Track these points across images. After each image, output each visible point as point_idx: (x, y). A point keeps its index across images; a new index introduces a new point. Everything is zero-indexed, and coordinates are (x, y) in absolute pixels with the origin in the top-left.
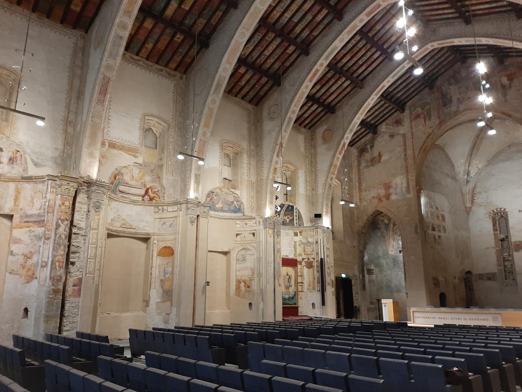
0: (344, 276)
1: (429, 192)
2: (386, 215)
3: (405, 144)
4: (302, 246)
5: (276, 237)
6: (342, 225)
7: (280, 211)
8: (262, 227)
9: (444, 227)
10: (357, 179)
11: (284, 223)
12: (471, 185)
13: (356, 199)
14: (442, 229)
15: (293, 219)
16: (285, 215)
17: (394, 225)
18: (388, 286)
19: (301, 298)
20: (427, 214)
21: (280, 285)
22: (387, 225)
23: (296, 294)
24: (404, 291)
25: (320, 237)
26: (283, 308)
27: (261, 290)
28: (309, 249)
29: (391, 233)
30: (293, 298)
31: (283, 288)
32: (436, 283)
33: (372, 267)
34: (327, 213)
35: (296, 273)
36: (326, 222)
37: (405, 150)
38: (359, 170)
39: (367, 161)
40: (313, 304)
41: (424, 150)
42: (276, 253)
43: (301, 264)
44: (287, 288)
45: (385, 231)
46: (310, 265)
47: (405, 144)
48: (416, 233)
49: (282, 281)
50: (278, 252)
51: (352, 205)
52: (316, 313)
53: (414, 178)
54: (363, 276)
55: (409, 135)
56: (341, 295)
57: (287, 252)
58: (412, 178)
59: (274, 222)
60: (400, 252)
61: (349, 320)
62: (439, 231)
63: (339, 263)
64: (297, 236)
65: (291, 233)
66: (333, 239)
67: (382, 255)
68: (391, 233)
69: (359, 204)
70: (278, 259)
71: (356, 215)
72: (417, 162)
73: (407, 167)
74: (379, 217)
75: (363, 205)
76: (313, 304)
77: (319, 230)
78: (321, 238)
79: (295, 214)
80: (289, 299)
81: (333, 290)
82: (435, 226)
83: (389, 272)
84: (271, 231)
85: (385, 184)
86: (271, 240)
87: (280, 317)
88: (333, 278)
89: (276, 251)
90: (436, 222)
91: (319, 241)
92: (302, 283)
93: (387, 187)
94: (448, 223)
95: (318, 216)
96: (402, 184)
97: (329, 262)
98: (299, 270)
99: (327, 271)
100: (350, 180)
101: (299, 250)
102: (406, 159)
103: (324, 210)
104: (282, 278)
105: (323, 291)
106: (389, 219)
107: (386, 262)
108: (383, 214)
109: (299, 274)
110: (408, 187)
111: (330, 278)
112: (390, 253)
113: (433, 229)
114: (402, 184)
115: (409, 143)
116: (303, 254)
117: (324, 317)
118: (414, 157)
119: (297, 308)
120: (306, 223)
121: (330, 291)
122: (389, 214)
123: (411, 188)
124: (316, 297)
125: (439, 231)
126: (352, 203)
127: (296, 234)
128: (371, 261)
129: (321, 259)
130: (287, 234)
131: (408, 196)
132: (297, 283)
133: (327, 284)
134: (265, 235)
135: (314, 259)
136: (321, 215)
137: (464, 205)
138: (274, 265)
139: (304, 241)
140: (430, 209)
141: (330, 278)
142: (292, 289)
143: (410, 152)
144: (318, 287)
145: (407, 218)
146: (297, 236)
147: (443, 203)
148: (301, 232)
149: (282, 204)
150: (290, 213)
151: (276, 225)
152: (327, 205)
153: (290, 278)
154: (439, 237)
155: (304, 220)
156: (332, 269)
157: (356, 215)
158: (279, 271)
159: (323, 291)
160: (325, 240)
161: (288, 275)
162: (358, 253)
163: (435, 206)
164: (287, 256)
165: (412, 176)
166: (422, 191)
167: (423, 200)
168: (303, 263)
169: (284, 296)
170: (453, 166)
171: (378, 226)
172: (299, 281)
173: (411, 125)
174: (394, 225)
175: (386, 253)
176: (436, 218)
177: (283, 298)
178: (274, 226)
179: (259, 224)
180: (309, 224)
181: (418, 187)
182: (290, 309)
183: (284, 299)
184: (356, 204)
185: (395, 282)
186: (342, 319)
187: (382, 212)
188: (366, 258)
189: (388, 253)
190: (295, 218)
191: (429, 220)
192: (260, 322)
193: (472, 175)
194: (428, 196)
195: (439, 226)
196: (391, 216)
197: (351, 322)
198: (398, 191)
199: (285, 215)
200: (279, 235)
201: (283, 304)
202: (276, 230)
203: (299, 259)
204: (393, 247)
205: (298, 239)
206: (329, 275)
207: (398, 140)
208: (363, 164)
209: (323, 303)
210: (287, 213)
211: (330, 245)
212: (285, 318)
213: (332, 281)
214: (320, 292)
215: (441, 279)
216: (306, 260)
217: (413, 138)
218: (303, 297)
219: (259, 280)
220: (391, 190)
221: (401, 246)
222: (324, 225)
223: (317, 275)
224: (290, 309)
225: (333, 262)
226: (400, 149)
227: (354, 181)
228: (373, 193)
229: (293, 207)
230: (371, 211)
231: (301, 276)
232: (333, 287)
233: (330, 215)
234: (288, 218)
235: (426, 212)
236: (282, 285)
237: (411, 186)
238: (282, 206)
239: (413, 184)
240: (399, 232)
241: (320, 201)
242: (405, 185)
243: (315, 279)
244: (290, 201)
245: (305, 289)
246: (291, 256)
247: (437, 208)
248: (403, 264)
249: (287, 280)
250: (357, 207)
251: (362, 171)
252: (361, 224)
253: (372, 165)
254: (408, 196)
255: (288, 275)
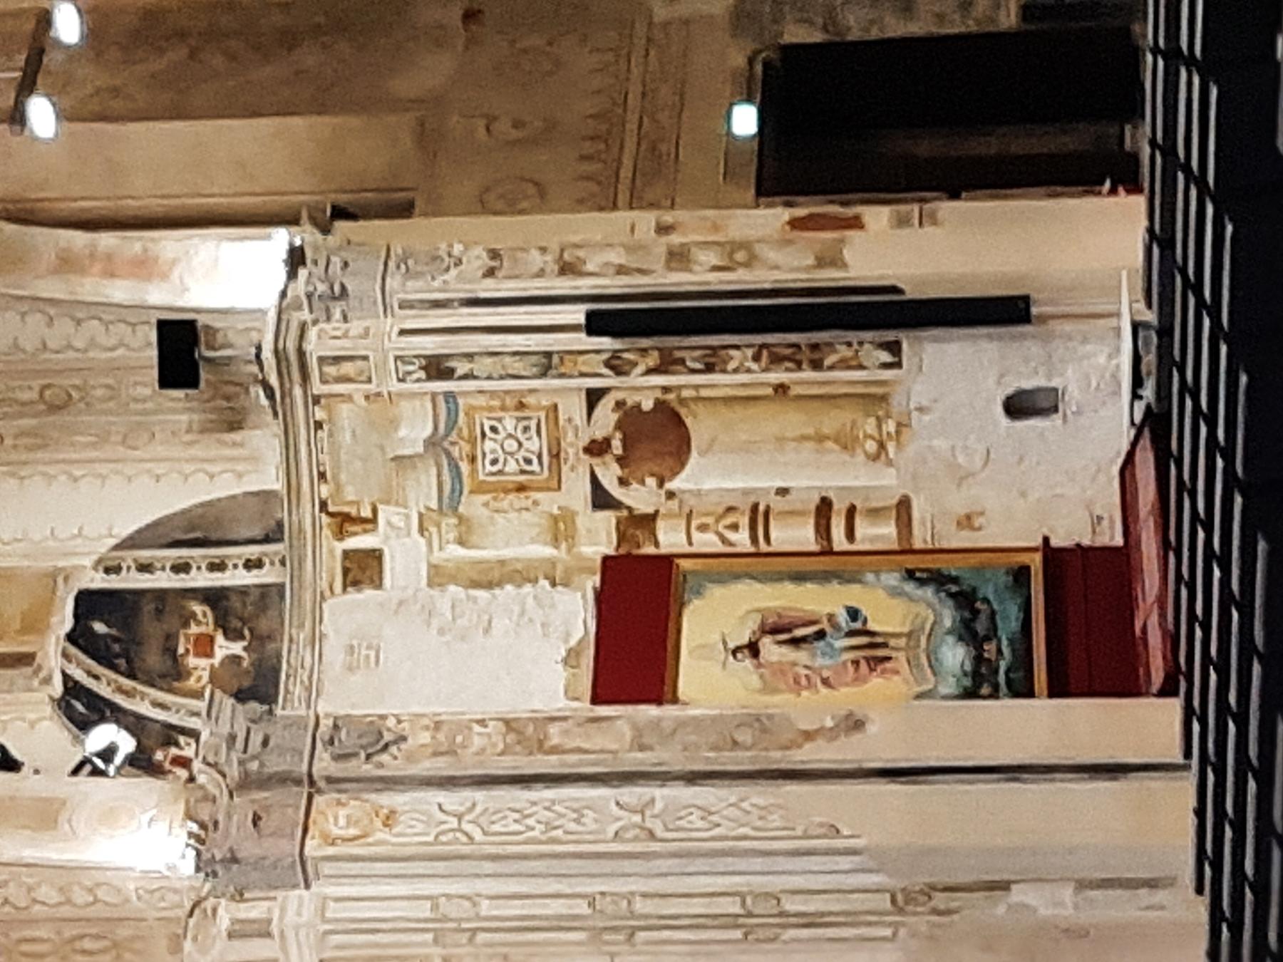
0: (745, 120)
4: (473, 505)
5: (390, 764)
6: (265, 125)
7: (135, 724)
8: (294, 908)
11: (257, 686)
15: (214, 597)
16: (172, 675)
19: (967, 522)
21: (855, 724)
23: (929, 573)
25: (376, 334)
26: (1053, 694)
27: (902, 901)
28: (509, 445)
30: (965, 600)
31: (879, 694)
34: (144, 268)
35: (728, 567)
36: (231, 278)
40: (1019, 406)
42: (549, 764)
43: (649, 521)
44: (873, 651)
46: (657, 437)
49: (813, 708)
50: (541, 746)
52: (1099, 378)
56: (925, 147)
57: (537, 650)
59: (247, 783)
61: (1152, 68)
63: (631, 166)
64: (375, 556)
65: (346, 614)
66: (404, 210)
70: (599, 740)
76: (1019, 406)
77: (314, 347)
78: (391, 325)
79: (163, 580)
80: (968, 633)
81: (877, 217)
84: (336, 816)
86: (421, 815)
87: (1153, 724)
88: (774, 217)
89: (526, 765)
91: (431, 345)
92: (824, 508)
95: (182, 350)
97: (621, 249)
98: (707, 542)
99: (702, 275)
101: (513, 535)
103: (120, 291)
104: (781, 702)
105: (893, 314)
109: (741, 539)
111: (769, 247)
116: (550, 502)
117: (1130, 305)
119: (1050, 553)
120: (249, 466)
121: (890, 247)
124: (953, 377)
127: (363, 569)
129: (595, 324)
130: (363, 655)
132: (826, 563)
133: (829, 277)
134: (378, 872)
135: (594, 397)
136: (163, 326)
138: (664, 778)
139: (424, 489)
141: (769, 247)
142: (890, 607)
144: (858, 361)
146: (375, 556)
148: (344, 522)
149: (64, 705)
150: (152, 629)
151: (275, 764)
152: (67, 264)
153: (778, 628)
155: (225, 487)
156: (693, 225)
158: (725, 731)
159: (893, 314)
160: (417, 290)
161: (753, 649)
164: (571, 658)
168: (641, 497)
169: (949, 686)
172: (796, 535)
177: (970, 693)
178: (285, 779)
179: (262, 930)
180: (263, 440)
182: (1059, 624)
183: (978, 683)
186: (1140, 140)
190: (201, 579)
192: (1200, 910)
197: (1172, 55)
199: (172, 675)
200: (377, 739)
201: (1023, 689)
202: (324, 764)
203: (598, 537)
205: (403, 551)
206: (738, 252)
209: (1006, 311)
210: (153, 659)
211: (458, 249)
212: (1157, 678)
213: (795, 224)
214: (907, 340)
216: (609, 475)
218: (958, 502)
219: (811, 921)
222: (268, 300)
223: (744, 369)
224: (1059, 624)
225: (623, 217)
229: (89, 603)
231: (759, 518)
232: (856, 223)
233: (168, 243)
234: (204, 646)
236: (846, 697)
238: (82, 708)
241: (32, 330)
243: (781, 389)
244: (35, 624)
245: (884, 482)
246: (575, 614)
249: (801, 656)
255: (753, 649)
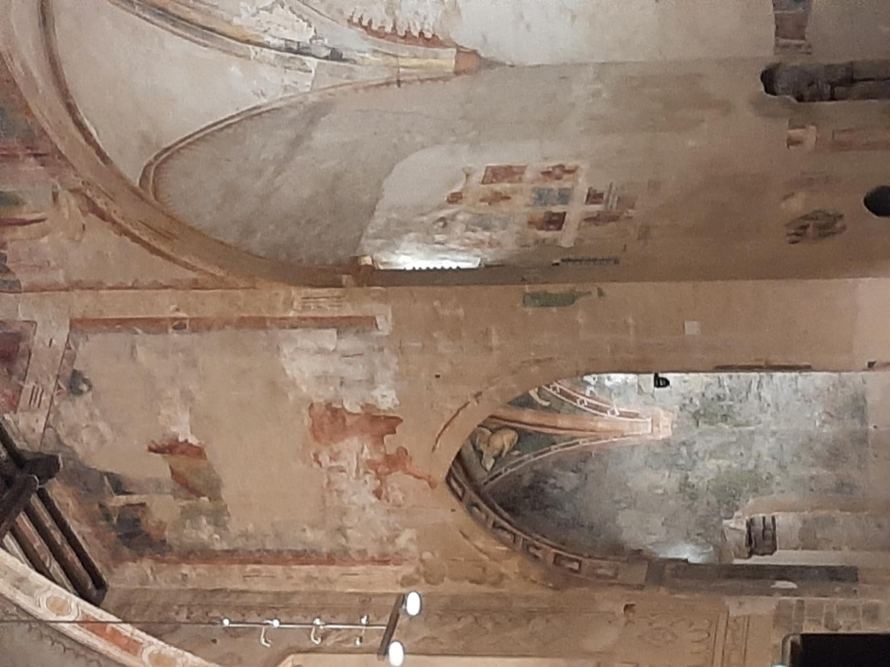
1: (370, 231)
2: (472, 438)
3: (124, 324)
9: (547, 173)
10: (278, 569)
12: (353, 42)
13: (381, 580)
14: (554, 185)
17: (525, 402)
18: (834, 455)
20: (479, 244)
22: (525, 438)
24: (856, 378)
29: (563, 421)
32: (818, 227)
33: (736, 525)
37: (154, 325)
38: (231, 556)
39: (192, 514)
41: (165, 236)
45: (554, 450)
47: (124, 324)
48: (570, 299)
51: (413, 604)
53: (297, 294)
54: (783, 572)
55: (83, 304)
58: (295, 300)
60: (661, 383)
62: (565, 197)
67: (677, 476)
68: (563, 421)
69: (408, 570)
71: (467, 587)
72: (220, 273)
73: (242, 323)
74: (480, 475)
75: (413, 548)
82: (540, 212)
83: (764, 447)
85: (316, 431)
90: (521, 205)
93: (330, 421)
94: (530, 155)
96: (322, 351)
100: (281, 603)
102: (199, 325)
106: (494, 424)
107: (712, 454)
108: (469, 452)
110: (341, 325)
112: (665, 432)
113: (556, 221)
114: (322, 351)
115: (115, 305)
118: (195, 285)
122: (469, 423)
123: (348, 310)
125: (565, 197)
126: (402, 600)
128: (706, 530)
131: (385, 326)
137: (446, 78)
140: (458, 229)
143: (166, 306)
145: (495, 341)
147: (426, 172)
154: (593, 197)
157: (467, 587)
162: (663, 591)
163: (440, 208)
165: (288, 303)
166: (368, 260)
167: (409, 259)
170: (254, 115)
171: (526, 481)
173: (32, 289)
174: (525, 402)
175: (667, 454)
176: (504, 206)
181: (345, 278)
184: (408, 582)
185: (815, 422)
187: (459, 456)
188: (689, 553)
189: (666, 443)
191: (506, 242)
193: (303, 35)
194: (393, 235)
195: (541, 197)
196: (478, 413)
198: (356, 371)
204: (636, 415)
207: (95, 355)
208: (204, 533)
215: (797, 205)
217: (96, 287)
220: (351, 405)
221: (631, 377)
226: (147, 350)
227: (288, 588)
228: (359, 493)
230: (447, 512)
235: (469, 247)
237: (331, 312)
239: (324, 302)
240: (564, 385)
242: (328, 338)
247: (455, 198)
248: (724, 375)
250: (427, 576)
251: (239, 543)
252: (512, 566)
253: (213, 489)
254: (385, 326)
